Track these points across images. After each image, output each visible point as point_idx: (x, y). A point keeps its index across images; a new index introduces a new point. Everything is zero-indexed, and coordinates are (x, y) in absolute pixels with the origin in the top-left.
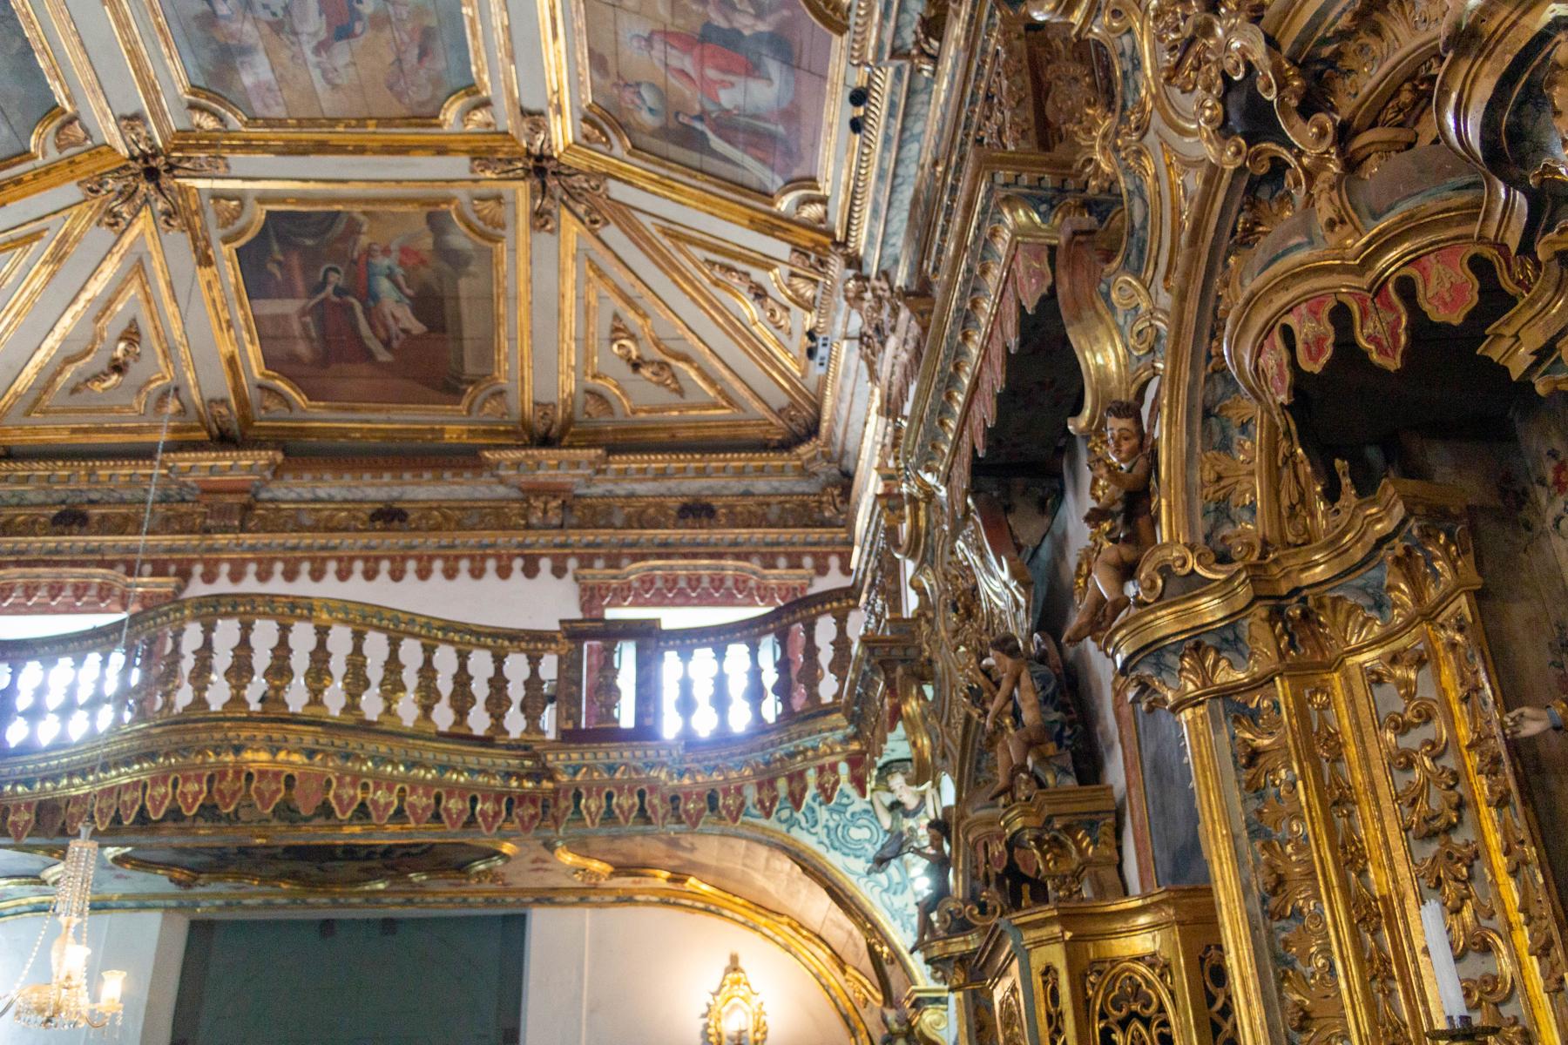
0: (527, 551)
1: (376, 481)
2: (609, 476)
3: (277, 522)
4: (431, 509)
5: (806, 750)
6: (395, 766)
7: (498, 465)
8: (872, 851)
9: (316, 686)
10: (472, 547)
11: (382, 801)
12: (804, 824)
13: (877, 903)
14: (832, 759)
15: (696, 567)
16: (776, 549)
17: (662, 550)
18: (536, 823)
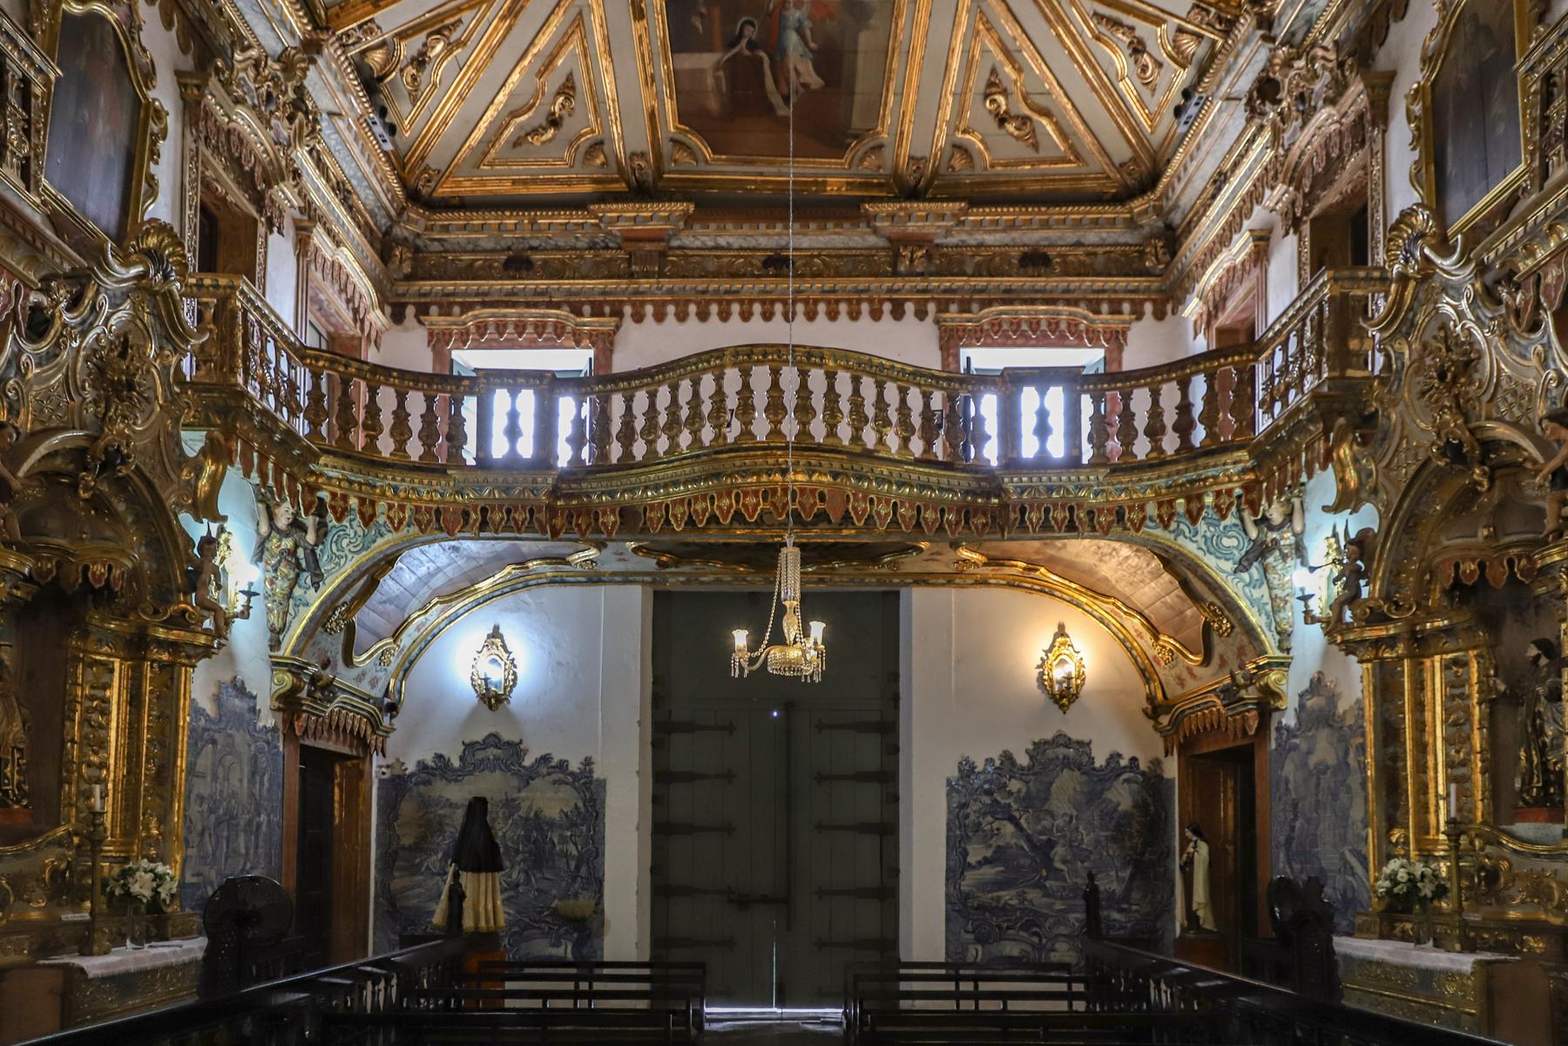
0: (895, 296)
1: (770, 231)
2: (966, 228)
3: (690, 266)
4: (813, 256)
5: (1207, 478)
6: (870, 482)
7: (875, 217)
8: (1238, 555)
9: (831, 421)
10: (849, 292)
11: (883, 512)
12: (1187, 534)
13: (1241, 594)
14: (1230, 485)
15: (1037, 312)
16: (1101, 296)
17: (1006, 296)
18: (988, 530)
